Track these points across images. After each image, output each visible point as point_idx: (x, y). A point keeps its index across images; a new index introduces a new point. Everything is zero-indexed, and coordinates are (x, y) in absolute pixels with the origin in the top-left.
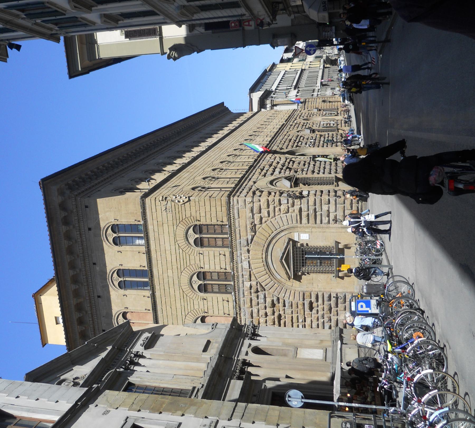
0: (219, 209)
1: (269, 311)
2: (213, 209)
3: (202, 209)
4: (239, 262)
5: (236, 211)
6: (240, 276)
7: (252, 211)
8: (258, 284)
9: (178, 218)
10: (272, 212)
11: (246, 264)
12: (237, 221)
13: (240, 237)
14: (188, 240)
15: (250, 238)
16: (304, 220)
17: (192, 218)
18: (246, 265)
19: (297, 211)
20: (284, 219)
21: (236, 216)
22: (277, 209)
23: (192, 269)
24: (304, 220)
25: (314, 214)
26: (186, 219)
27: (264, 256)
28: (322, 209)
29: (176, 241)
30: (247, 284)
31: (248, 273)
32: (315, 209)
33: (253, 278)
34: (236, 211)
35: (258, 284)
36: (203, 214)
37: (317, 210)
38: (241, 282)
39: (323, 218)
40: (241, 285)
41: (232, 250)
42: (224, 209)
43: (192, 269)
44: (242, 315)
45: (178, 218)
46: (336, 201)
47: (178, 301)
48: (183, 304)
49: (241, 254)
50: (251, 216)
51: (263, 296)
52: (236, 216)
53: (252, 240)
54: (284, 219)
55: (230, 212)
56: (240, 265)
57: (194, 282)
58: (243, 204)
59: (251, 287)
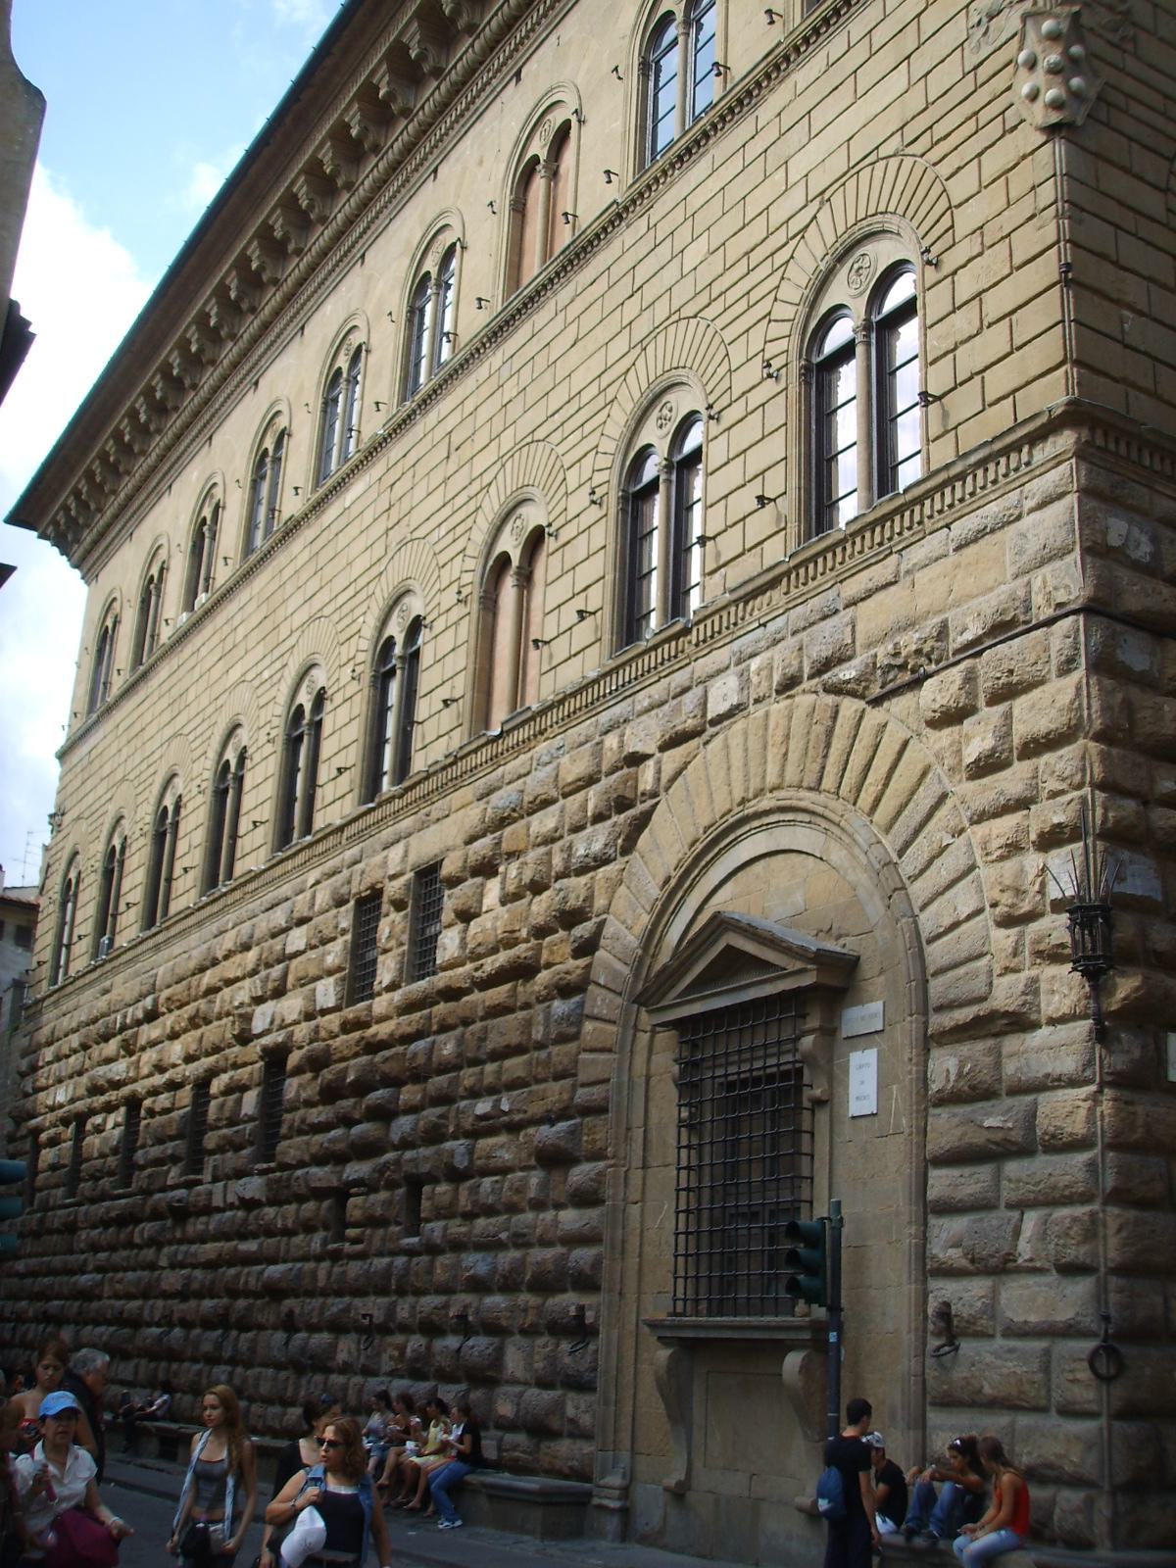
0: (1000, 380)
1: (540, 907)
2: (996, 340)
3: (996, 261)
4: (735, 646)
5: (993, 510)
6: (680, 679)
7: (1002, 629)
8: (650, 802)
9: (940, 130)
10: (991, 795)
11: (725, 697)
12: (933, 544)
13: (853, 603)
14: (841, 259)
15: (847, 672)
16: (945, 1065)
17: (946, 222)
18: (723, 694)
19: (1005, 994)
20: (963, 899)
21: (963, 528)
22: (1006, 825)
23: (711, 370)
24: (945, 1065)
25: (980, 1139)
26: (937, 189)
27: (765, 803)
28: (1021, 1206)
29: (827, 195)
30: (643, 736)
31: (690, 723)
32: (1024, 1150)
33: (672, 759)
34: (993, 510)
35: (650, 802)
36: (966, 286)
37: (1012, 1168)
38: (656, 691)
39: (958, 1225)
40: (643, 700)
41: (787, 573)
42: (1000, 418)
43: (711, 370)
44: (542, 748)
45: (940, 130)
46: (1070, 1331)
47: (596, 365)
48: (586, 397)
49: (776, 642)
50: (969, 636)
51: (597, 847)
52: (963, 528)
53: (836, 690)
54: (963, 899)
55: (982, 463)
56: (721, 656)
57: (665, 411)
58: (1033, 547)
59: (636, 759)
